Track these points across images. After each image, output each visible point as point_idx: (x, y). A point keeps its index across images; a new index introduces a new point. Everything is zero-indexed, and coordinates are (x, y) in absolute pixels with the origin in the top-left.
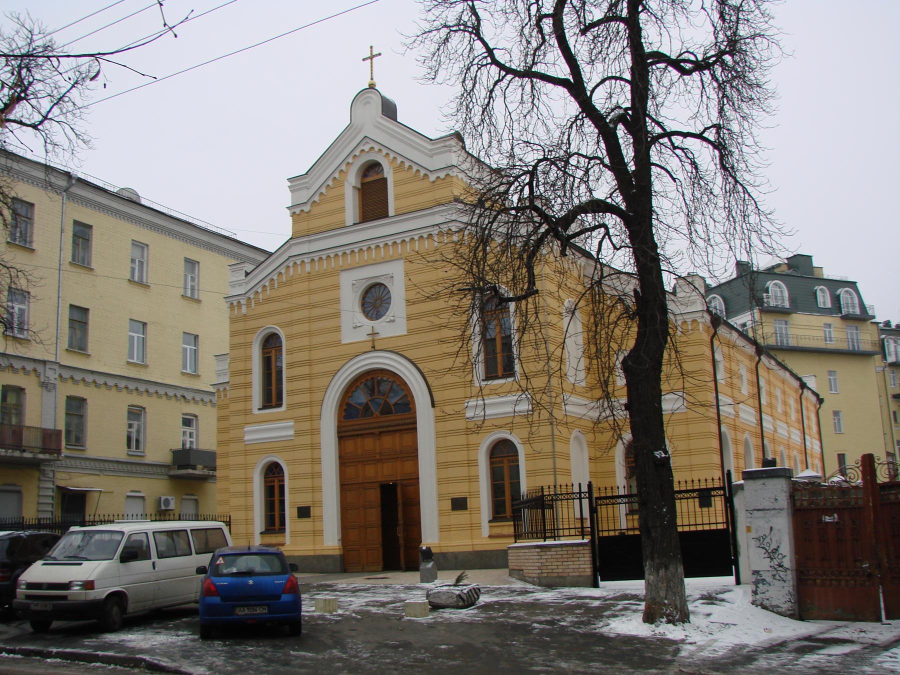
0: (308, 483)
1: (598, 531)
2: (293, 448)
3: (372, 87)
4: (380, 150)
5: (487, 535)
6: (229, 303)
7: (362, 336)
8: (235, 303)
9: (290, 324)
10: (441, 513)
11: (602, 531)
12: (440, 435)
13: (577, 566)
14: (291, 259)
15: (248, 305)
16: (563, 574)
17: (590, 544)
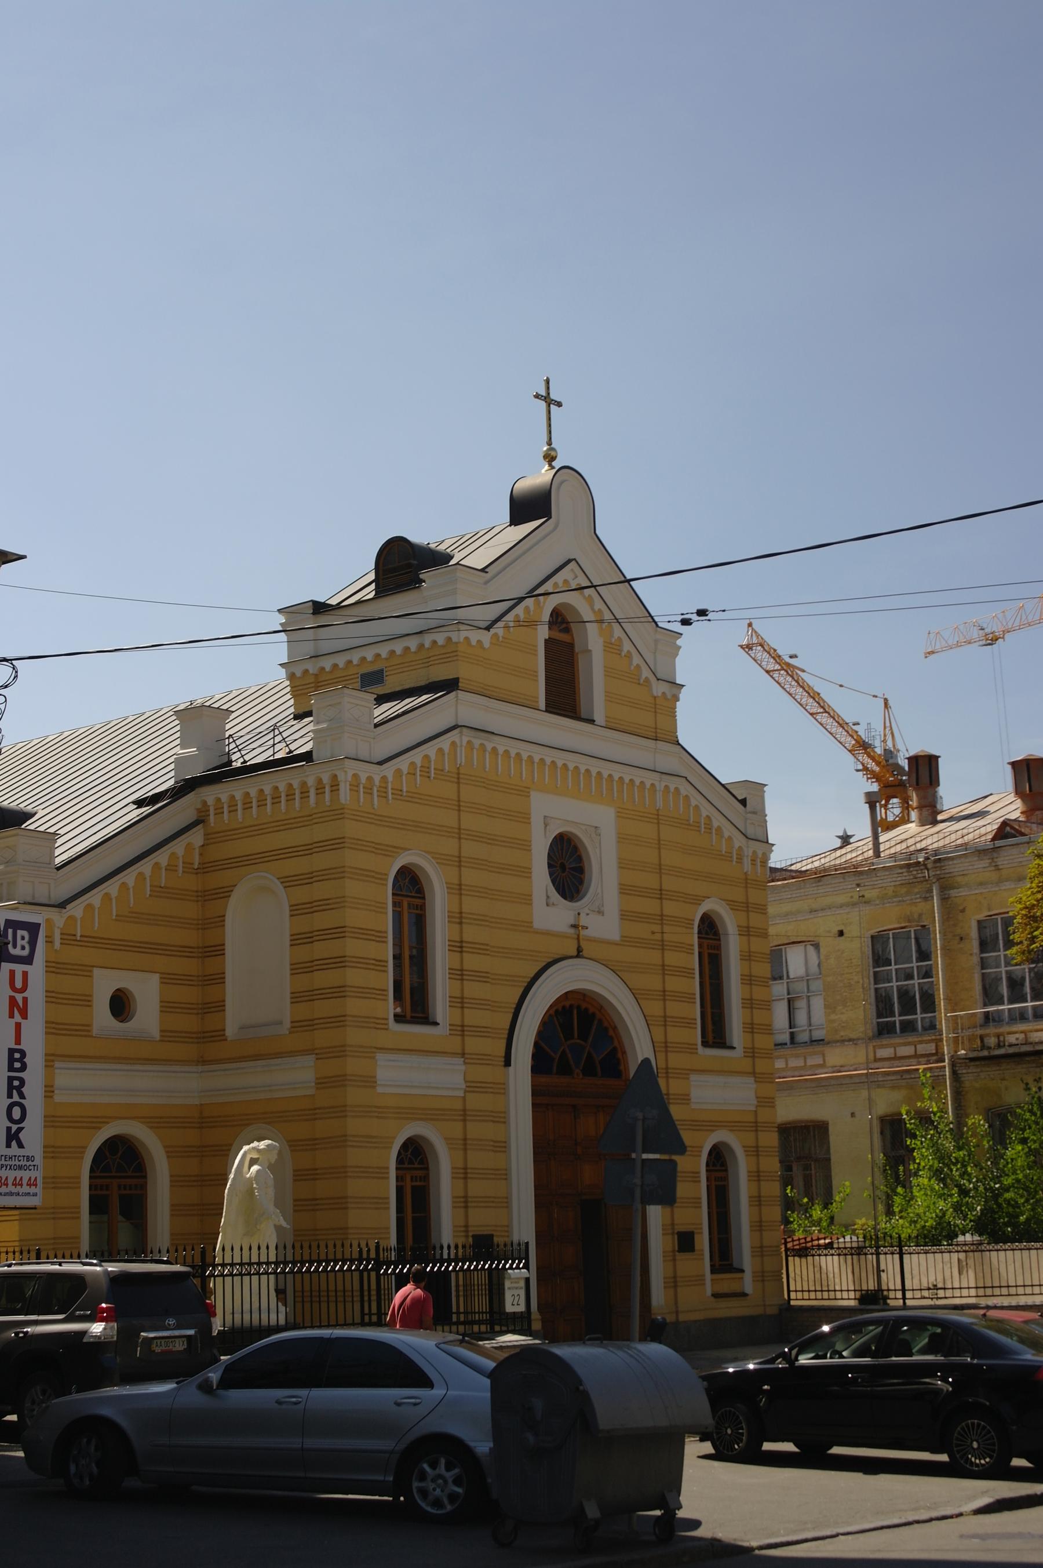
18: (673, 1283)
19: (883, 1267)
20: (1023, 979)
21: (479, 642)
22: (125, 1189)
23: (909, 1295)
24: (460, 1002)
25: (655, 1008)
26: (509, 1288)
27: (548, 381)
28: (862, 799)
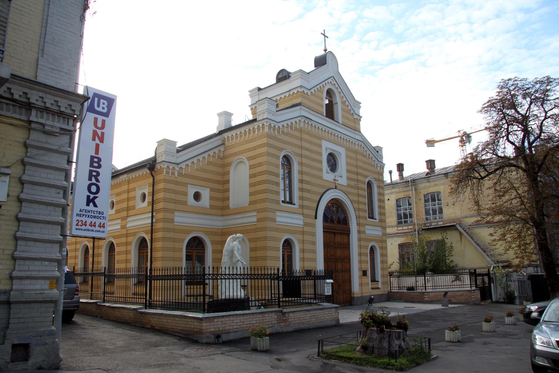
8: (273, 125)
14: (303, 117)
18: (361, 285)
19: (417, 280)
20: (436, 209)
21: (307, 93)
22: (198, 253)
23: (427, 288)
24: (301, 198)
25: (356, 206)
26: (326, 286)
27: (324, 31)
28: (388, 172)
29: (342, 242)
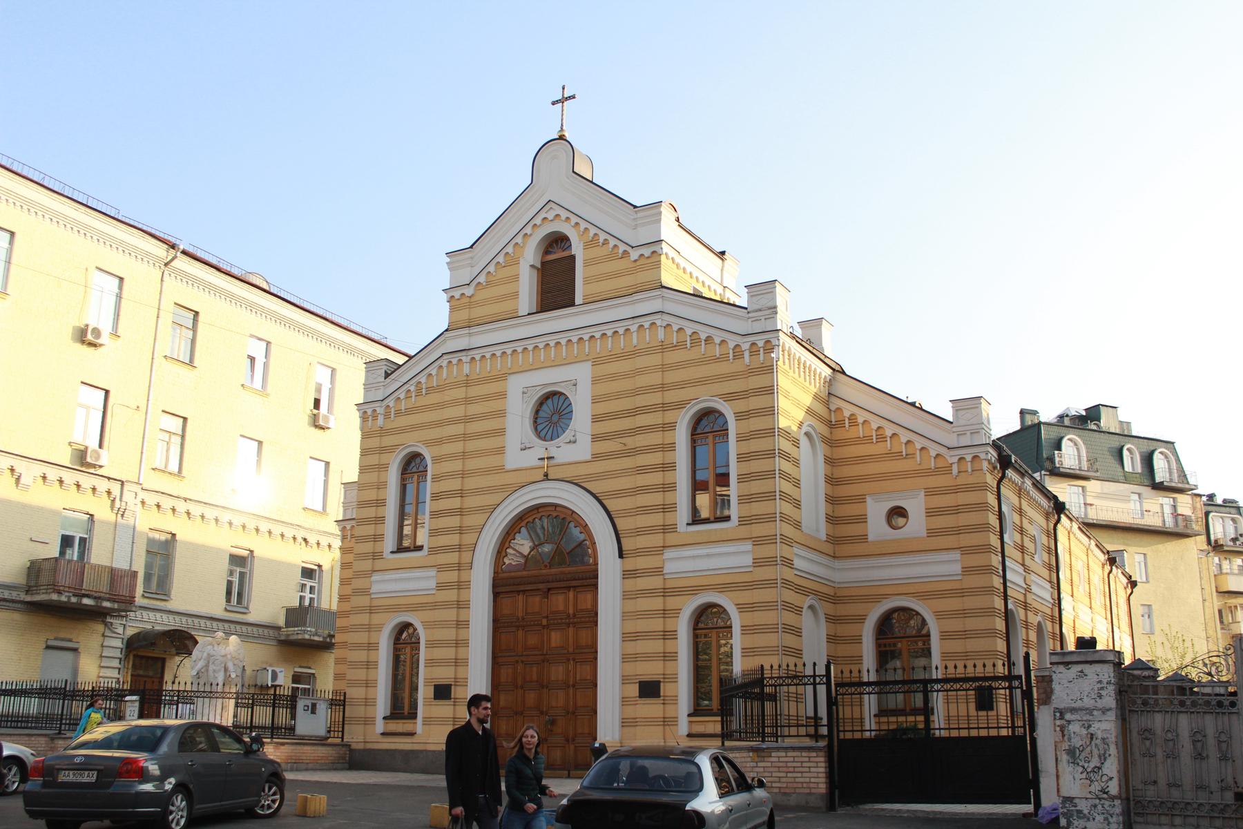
0: (449, 653)
1: (838, 731)
2: (435, 606)
3: (562, 138)
4: (568, 218)
5: (686, 733)
6: (362, 411)
7: (530, 459)
8: (369, 411)
9: (439, 442)
10: (625, 701)
11: (844, 731)
12: (627, 596)
13: (807, 780)
14: (445, 357)
15: (387, 415)
16: (788, 791)
17: (826, 749)
29: (571, 612)
